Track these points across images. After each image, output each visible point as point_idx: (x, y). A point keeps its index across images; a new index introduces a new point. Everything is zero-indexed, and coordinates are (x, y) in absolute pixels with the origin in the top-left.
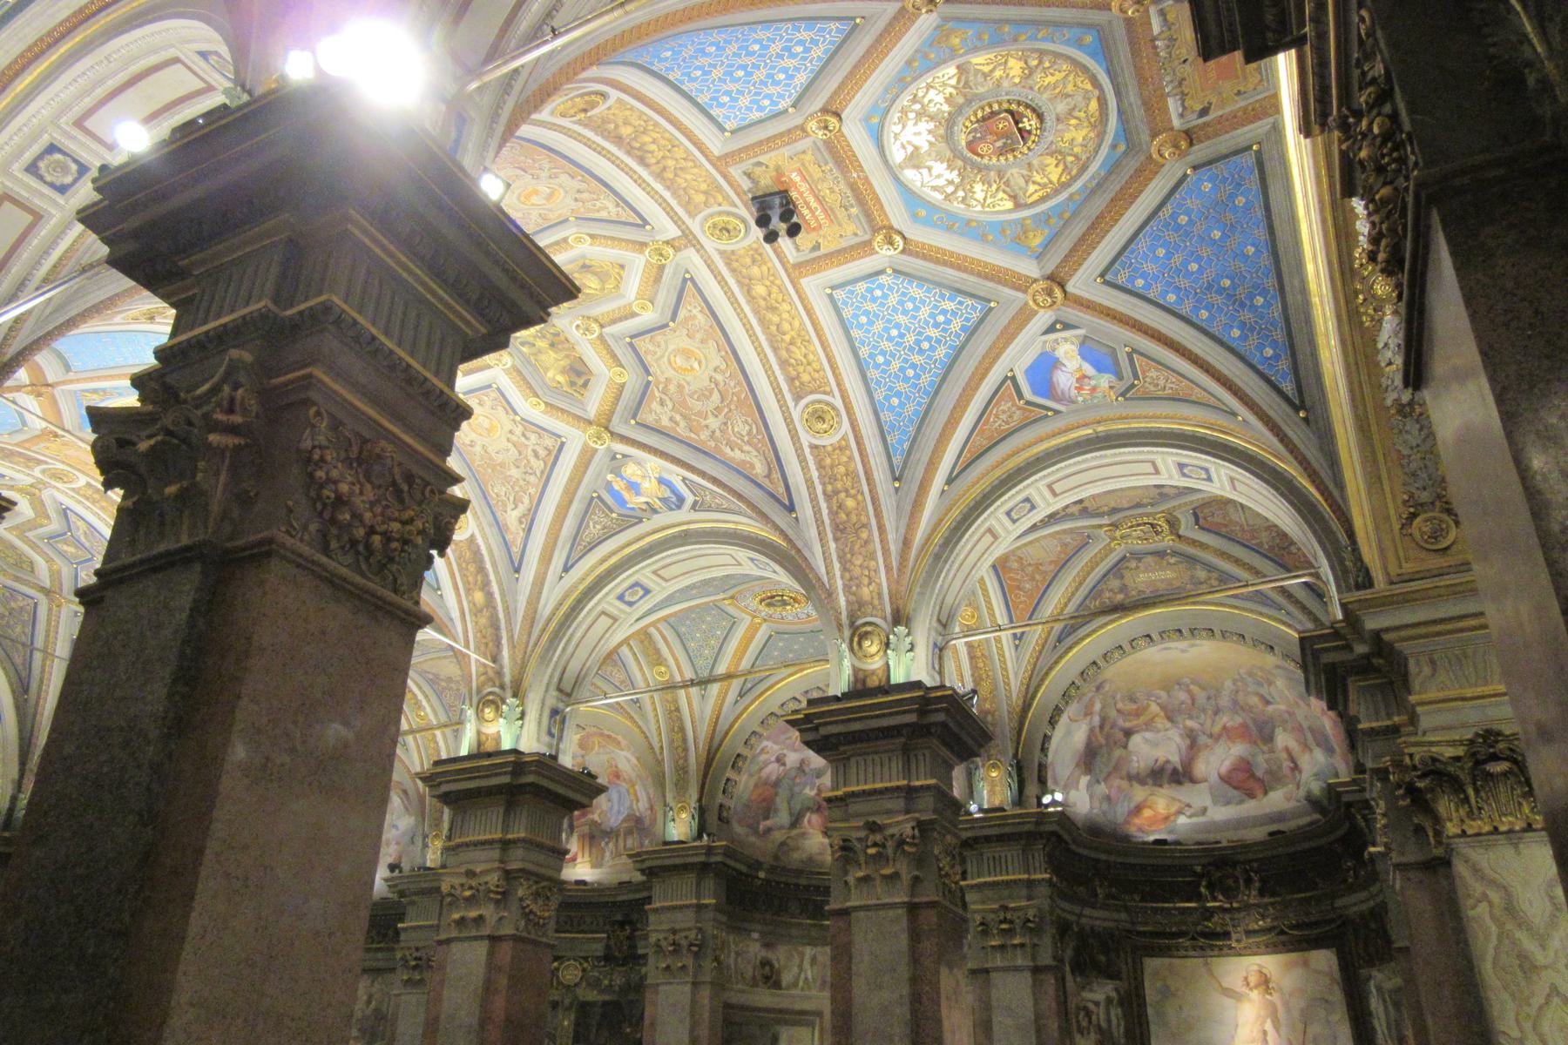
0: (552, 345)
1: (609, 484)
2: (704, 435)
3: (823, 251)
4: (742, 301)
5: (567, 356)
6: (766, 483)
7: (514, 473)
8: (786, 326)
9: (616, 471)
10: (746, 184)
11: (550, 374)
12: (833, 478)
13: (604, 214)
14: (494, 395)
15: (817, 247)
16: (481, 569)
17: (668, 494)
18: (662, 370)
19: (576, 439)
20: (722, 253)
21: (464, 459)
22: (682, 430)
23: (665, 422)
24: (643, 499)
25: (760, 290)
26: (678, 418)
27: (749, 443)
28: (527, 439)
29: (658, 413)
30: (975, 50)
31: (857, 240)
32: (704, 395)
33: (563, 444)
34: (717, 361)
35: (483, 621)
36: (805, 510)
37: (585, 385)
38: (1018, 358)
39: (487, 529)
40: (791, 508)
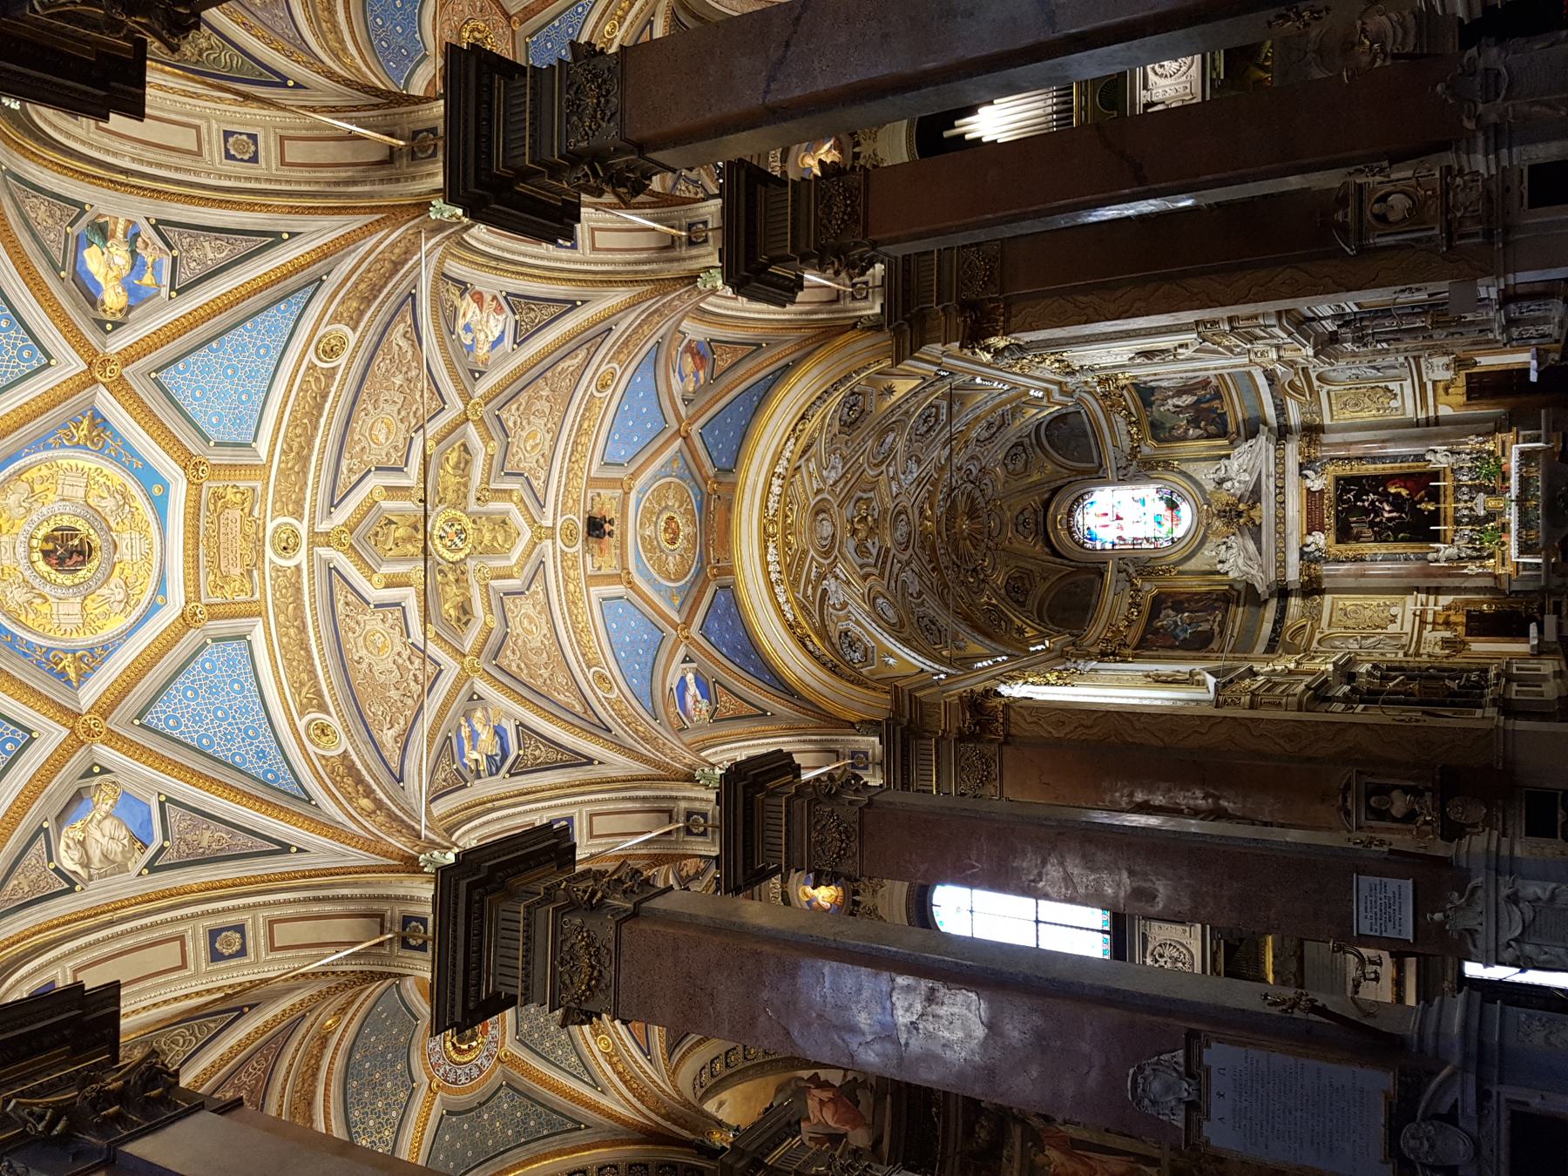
0: (457, 581)
1: (460, 725)
2: (540, 682)
3: (603, 572)
4: (562, 591)
5: (463, 594)
6: (585, 716)
7: (393, 694)
8: (580, 619)
9: (468, 715)
10: (589, 508)
11: (446, 607)
12: (623, 717)
13: (535, 483)
14: (398, 614)
15: (599, 569)
16: (360, 780)
17: (497, 750)
18: (516, 628)
19: (451, 668)
20: (562, 551)
21: (347, 676)
22: (524, 676)
23: (514, 668)
24: (475, 755)
25: (571, 587)
26: (523, 666)
27: (568, 690)
28: (411, 663)
29: (510, 659)
30: (676, 476)
31: (615, 572)
32: (538, 653)
33: (441, 671)
34: (545, 631)
35: (381, 818)
36: (616, 730)
37: (466, 624)
38: (673, 681)
39: (361, 746)
40: (610, 731)
